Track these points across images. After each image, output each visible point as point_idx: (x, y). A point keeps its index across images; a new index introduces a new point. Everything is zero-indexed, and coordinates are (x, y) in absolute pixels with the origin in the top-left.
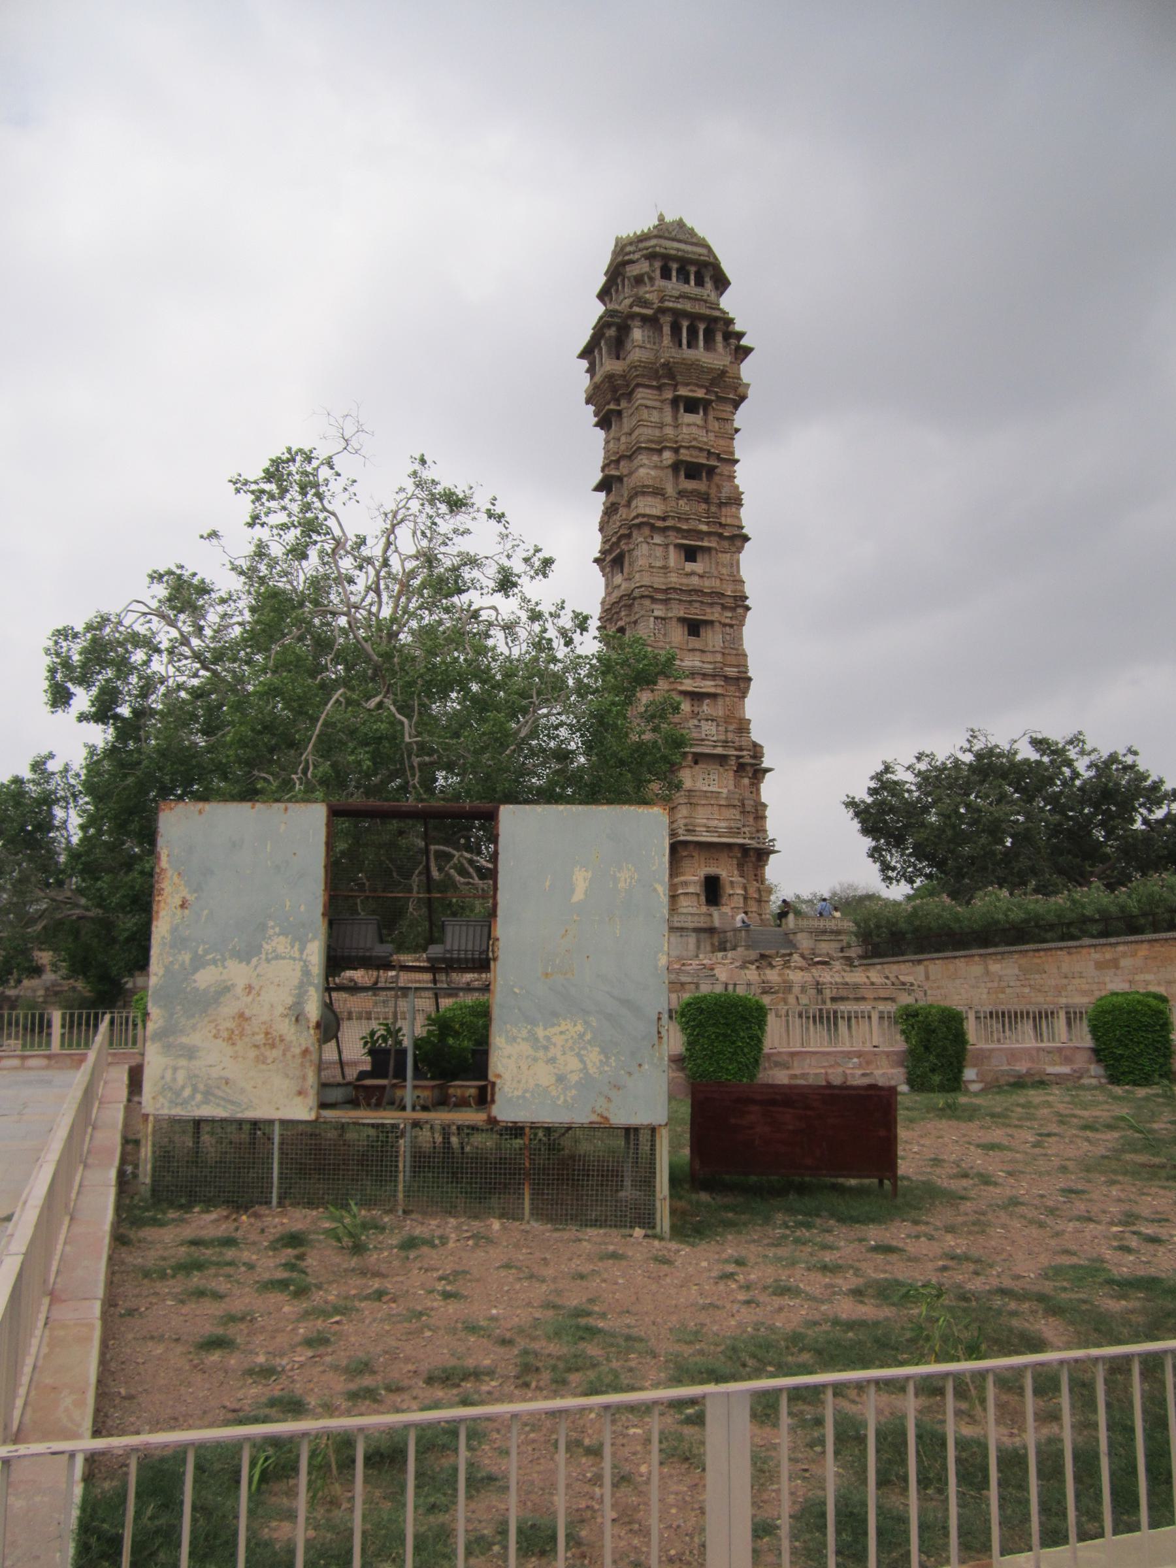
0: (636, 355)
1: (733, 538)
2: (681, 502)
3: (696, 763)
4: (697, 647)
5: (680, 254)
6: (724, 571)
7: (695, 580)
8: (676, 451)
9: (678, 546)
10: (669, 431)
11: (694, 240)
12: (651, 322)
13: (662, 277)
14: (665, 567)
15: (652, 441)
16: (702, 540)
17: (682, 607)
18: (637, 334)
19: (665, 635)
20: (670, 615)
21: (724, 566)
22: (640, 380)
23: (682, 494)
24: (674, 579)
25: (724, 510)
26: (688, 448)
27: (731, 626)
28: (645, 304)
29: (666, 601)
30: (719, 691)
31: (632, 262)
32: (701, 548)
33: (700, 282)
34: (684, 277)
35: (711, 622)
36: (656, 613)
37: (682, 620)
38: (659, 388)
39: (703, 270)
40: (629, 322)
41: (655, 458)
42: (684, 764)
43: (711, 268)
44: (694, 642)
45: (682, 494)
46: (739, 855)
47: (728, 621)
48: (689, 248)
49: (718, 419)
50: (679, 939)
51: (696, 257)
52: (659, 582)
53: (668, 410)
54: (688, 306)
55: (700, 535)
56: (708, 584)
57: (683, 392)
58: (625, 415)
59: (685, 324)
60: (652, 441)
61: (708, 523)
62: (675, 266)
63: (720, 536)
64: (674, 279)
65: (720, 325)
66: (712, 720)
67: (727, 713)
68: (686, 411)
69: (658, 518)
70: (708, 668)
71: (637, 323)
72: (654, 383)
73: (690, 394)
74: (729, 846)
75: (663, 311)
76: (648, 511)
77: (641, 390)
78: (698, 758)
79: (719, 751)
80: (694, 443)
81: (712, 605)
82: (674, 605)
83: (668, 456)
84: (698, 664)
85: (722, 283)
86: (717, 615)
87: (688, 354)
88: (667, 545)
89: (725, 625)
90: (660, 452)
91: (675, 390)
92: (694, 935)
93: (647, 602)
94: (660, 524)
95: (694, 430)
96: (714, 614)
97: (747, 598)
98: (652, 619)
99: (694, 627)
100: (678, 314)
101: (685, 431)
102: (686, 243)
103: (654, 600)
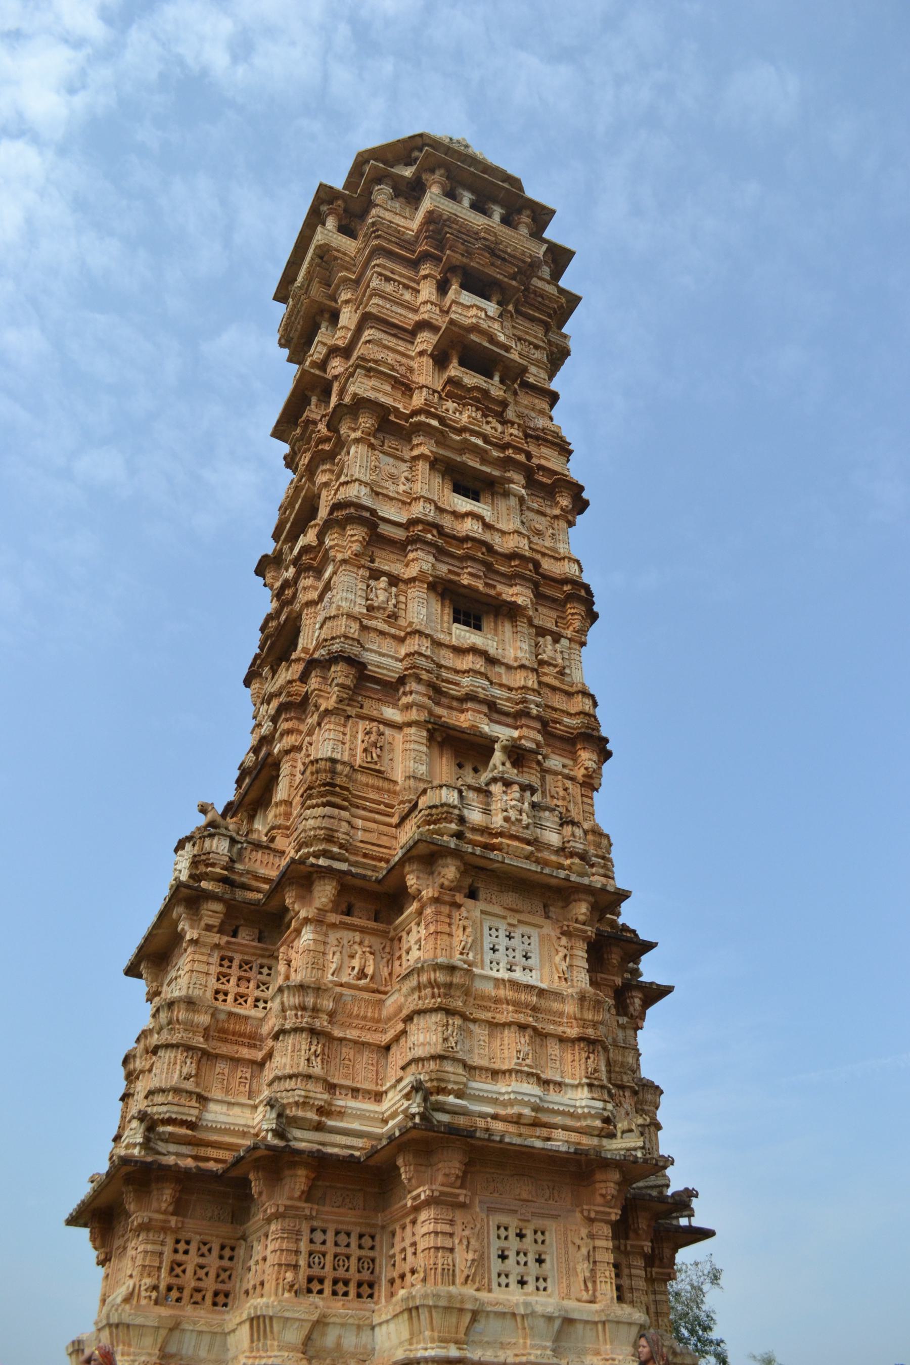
3: (472, 895)
35: (510, 612)
81: (511, 579)
89: (541, 632)
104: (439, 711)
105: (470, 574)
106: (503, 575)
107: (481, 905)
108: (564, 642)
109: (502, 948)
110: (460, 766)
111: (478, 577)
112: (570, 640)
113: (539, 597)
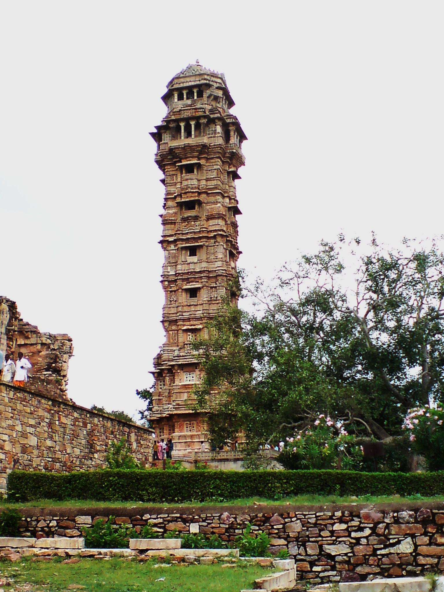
4: (192, 303)
23: (184, 220)
26: (186, 193)
27: (216, 287)
33: (200, 95)
44: (193, 301)
45: (184, 220)
57: (184, 163)
59: (182, 124)
62: (185, 92)
64: (185, 99)
80: (190, 190)
89: (212, 288)
99: (193, 293)
108: (218, 288)
113: (209, 278)
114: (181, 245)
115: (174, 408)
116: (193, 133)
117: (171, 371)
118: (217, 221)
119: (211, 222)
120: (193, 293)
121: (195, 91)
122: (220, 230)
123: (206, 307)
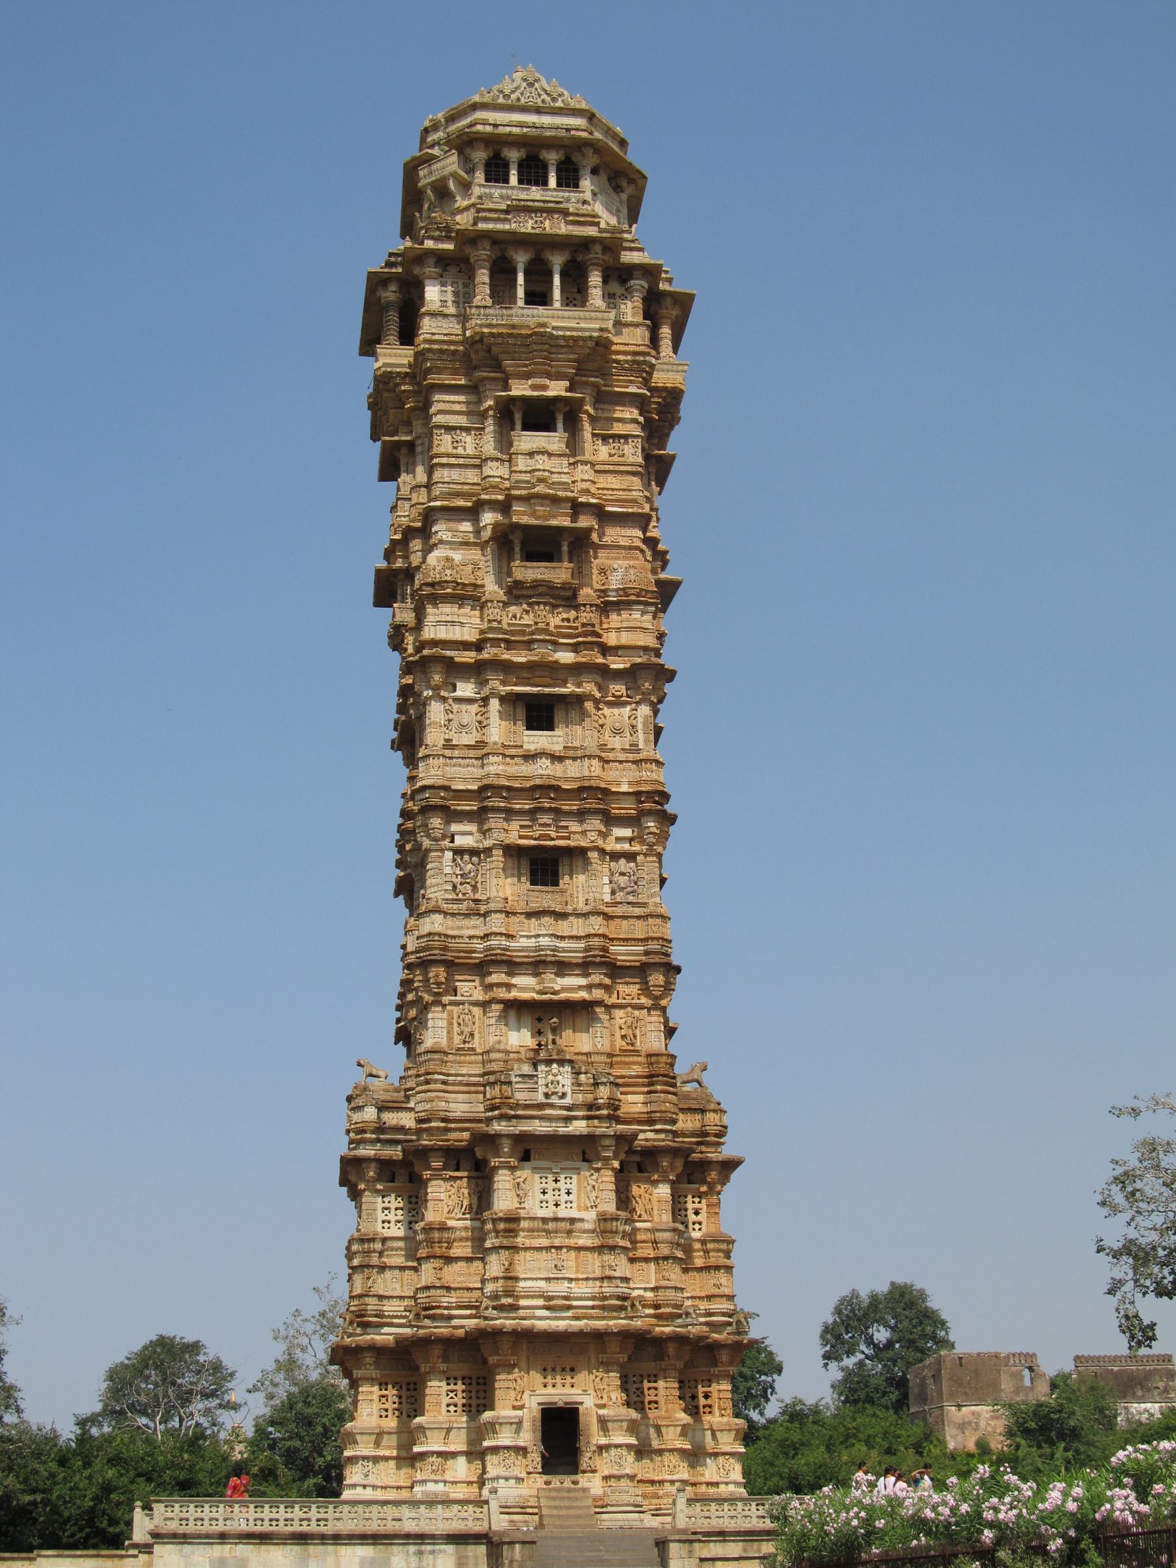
0: (428, 327)
1: (630, 675)
2: (513, 609)
3: (526, 1157)
5: (533, 132)
6: (616, 743)
7: (543, 769)
8: (504, 507)
9: (509, 700)
10: (495, 470)
11: (559, 104)
12: (455, 266)
13: (487, 180)
14: (480, 744)
15: (458, 495)
16: (564, 684)
17: (515, 825)
18: (433, 293)
19: (475, 888)
20: (488, 843)
21: (617, 732)
22: (434, 379)
24: (497, 769)
25: (614, 616)
27: (631, 857)
28: (447, 233)
29: (479, 816)
30: (598, 994)
31: (434, 157)
32: (562, 697)
33: (569, 179)
34: (533, 173)
35: (583, 851)
36: (460, 841)
37: (513, 852)
38: (474, 389)
39: (576, 158)
40: (416, 271)
41: (466, 526)
42: (495, 1161)
43: (589, 152)
44: (545, 898)
45: (517, 593)
46: (623, 1358)
47: (626, 846)
48: (546, 120)
49: (605, 439)
50: (413, 1560)
51: (563, 133)
52: (464, 775)
53: (490, 426)
54: (527, 226)
55: (556, 672)
56: (571, 773)
57: (519, 389)
58: (419, 449)
59: (521, 259)
60: (458, 495)
61: (575, 648)
62: (514, 155)
63: (605, 673)
64: (514, 179)
65: (597, 251)
66: (561, 1062)
67: (620, 1043)
68: (525, 428)
69: (465, 646)
70: (572, 950)
71: (430, 270)
72: (463, 382)
73: (535, 394)
74: (599, 1336)
75: (471, 239)
76: (442, 633)
77: (437, 397)
78: (528, 1149)
79: (579, 1127)
80: (540, 489)
81: (581, 815)
82: (495, 822)
83: (489, 518)
84: (545, 941)
85: (623, 181)
86: (592, 836)
87: (524, 315)
88: (485, 701)
89: (615, 856)
90: (473, 513)
91: (507, 388)
92: (450, 1549)
93: (436, 822)
94: (468, 657)
95: (541, 462)
96: (582, 833)
97: (665, 796)
98: (449, 855)
99: (544, 865)
100: (503, 243)
101: (521, 467)
102: (538, 111)
103: (451, 815)
104: (515, 980)
105: (541, 825)
106: (570, 814)
107: (534, 1163)
108: (640, 858)
109: (550, 1192)
110: (539, 1020)
111: (549, 825)
112: (646, 855)
114: (497, 684)
115: (494, 1308)
116: (557, 294)
117: (474, 1160)
118: (636, 615)
119: (614, 619)
120: (544, 865)
121: (552, 158)
122: (645, 649)
123: (596, 925)
